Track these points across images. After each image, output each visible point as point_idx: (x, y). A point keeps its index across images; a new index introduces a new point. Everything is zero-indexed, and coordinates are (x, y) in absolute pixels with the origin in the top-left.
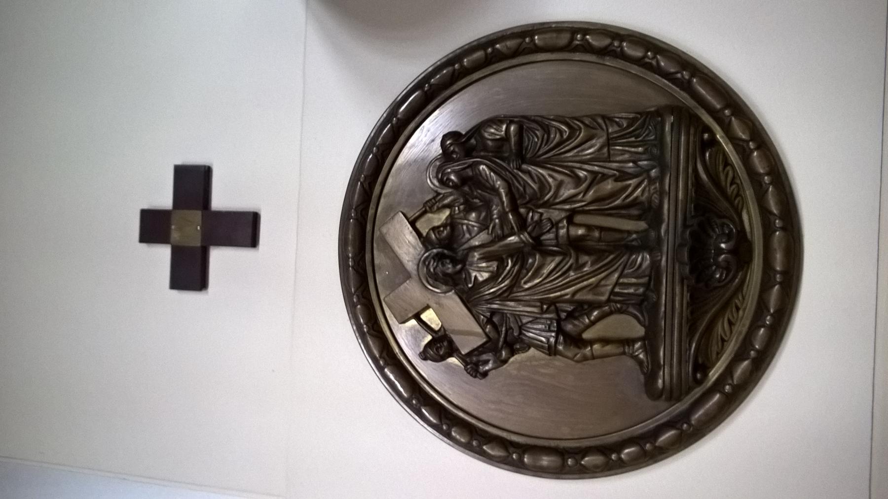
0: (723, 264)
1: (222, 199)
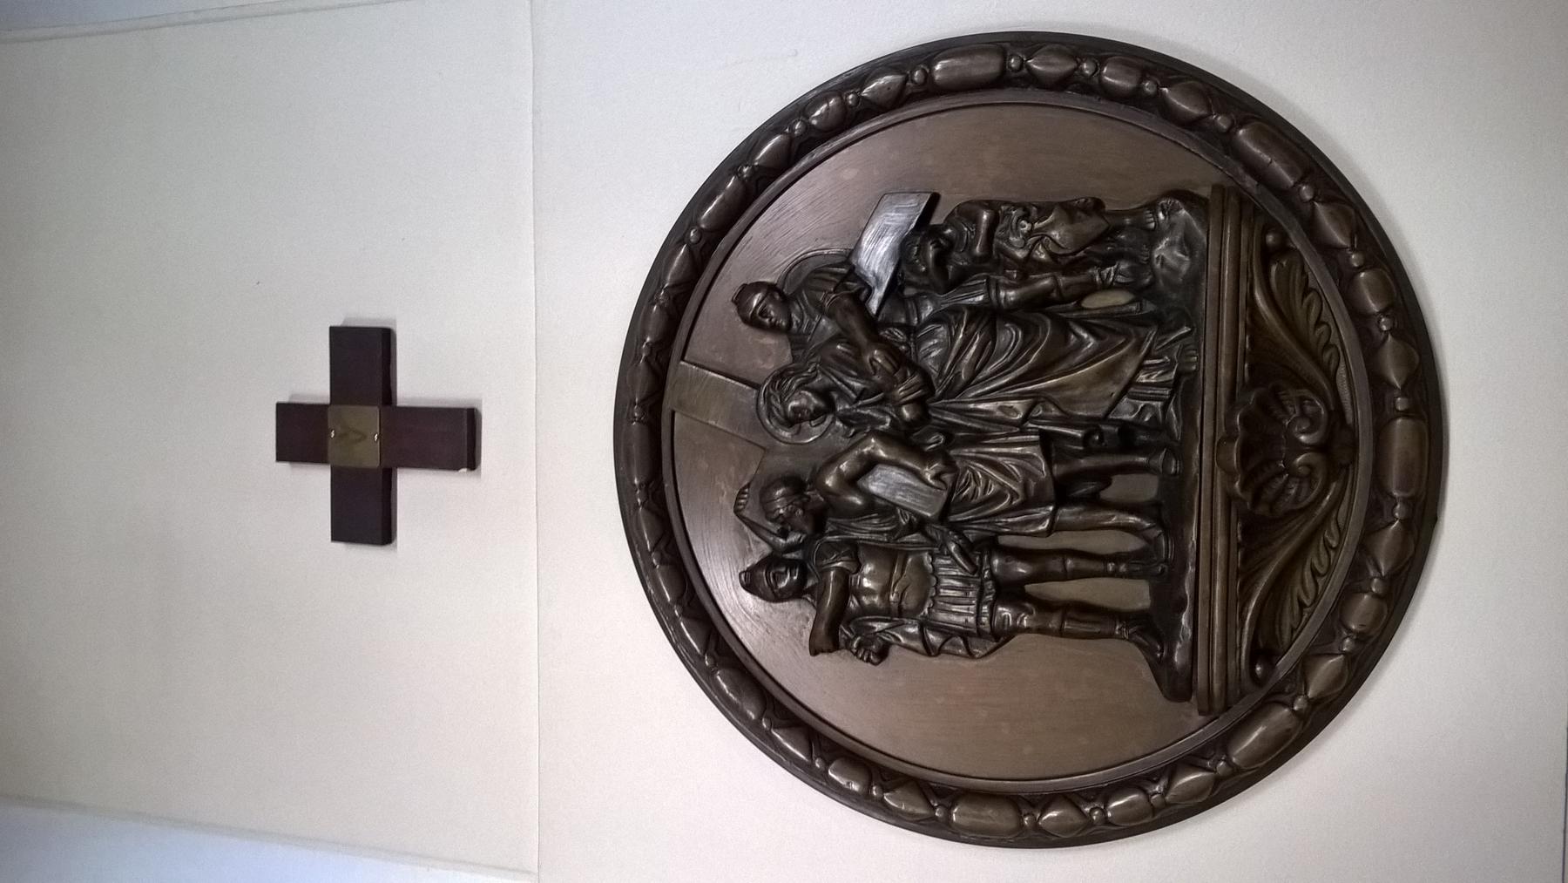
0: (1303, 471)
1: (415, 384)
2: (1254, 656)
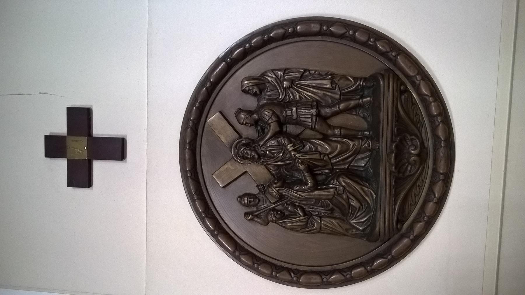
1: (101, 128)
2: (398, 221)
